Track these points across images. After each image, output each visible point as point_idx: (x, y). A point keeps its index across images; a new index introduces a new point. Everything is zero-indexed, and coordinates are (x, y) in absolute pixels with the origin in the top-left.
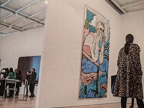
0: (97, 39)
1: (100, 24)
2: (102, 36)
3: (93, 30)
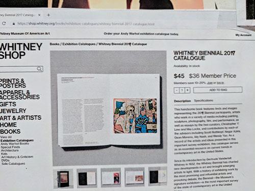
3: (124, 113)
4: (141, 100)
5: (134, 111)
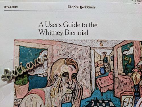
0: (53, 99)
1: (63, 62)
2: (69, 88)
4: (98, 45)
5: (74, 76)
